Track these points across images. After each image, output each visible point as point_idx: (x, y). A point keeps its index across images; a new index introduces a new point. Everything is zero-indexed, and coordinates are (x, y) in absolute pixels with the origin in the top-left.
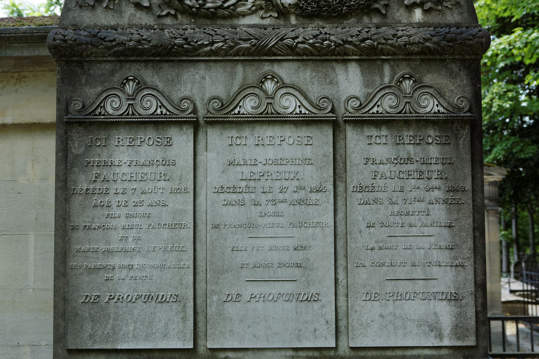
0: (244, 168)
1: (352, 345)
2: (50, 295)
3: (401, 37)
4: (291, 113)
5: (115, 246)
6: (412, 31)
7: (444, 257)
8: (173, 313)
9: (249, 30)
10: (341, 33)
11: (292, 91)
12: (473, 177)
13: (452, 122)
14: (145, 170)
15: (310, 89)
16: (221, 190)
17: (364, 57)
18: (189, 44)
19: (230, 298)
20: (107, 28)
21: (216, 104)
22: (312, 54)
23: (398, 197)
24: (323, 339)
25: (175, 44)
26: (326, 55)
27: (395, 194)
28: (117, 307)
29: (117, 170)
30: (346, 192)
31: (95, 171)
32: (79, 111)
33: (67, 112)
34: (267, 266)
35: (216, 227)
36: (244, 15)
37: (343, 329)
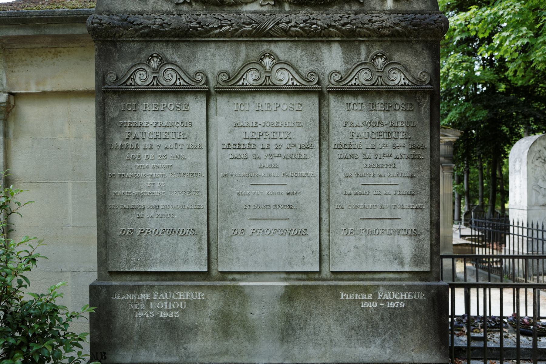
0: (247, 129)
1: (332, 269)
3: (375, 22)
4: (285, 85)
5: (145, 190)
6: (385, 17)
7: (407, 201)
8: (192, 244)
10: (326, 19)
11: (285, 66)
12: (431, 137)
13: (416, 92)
14: (168, 130)
15: (300, 65)
16: (228, 147)
17: (345, 39)
18: (202, 27)
19: (236, 233)
20: (134, 13)
21: (225, 77)
22: (302, 36)
23: (370, 153)
24: (310, 265)
25: (191, 28)
26: (314, 37)
27: (368, 151)
28: (147, 239)
29: (146, 130)
30: (329, 149)
31: (128, 130)
32: (114, 82)
33: (104, 83)
34: (265, 208)
35: (225, 176)
37: (325, 257)
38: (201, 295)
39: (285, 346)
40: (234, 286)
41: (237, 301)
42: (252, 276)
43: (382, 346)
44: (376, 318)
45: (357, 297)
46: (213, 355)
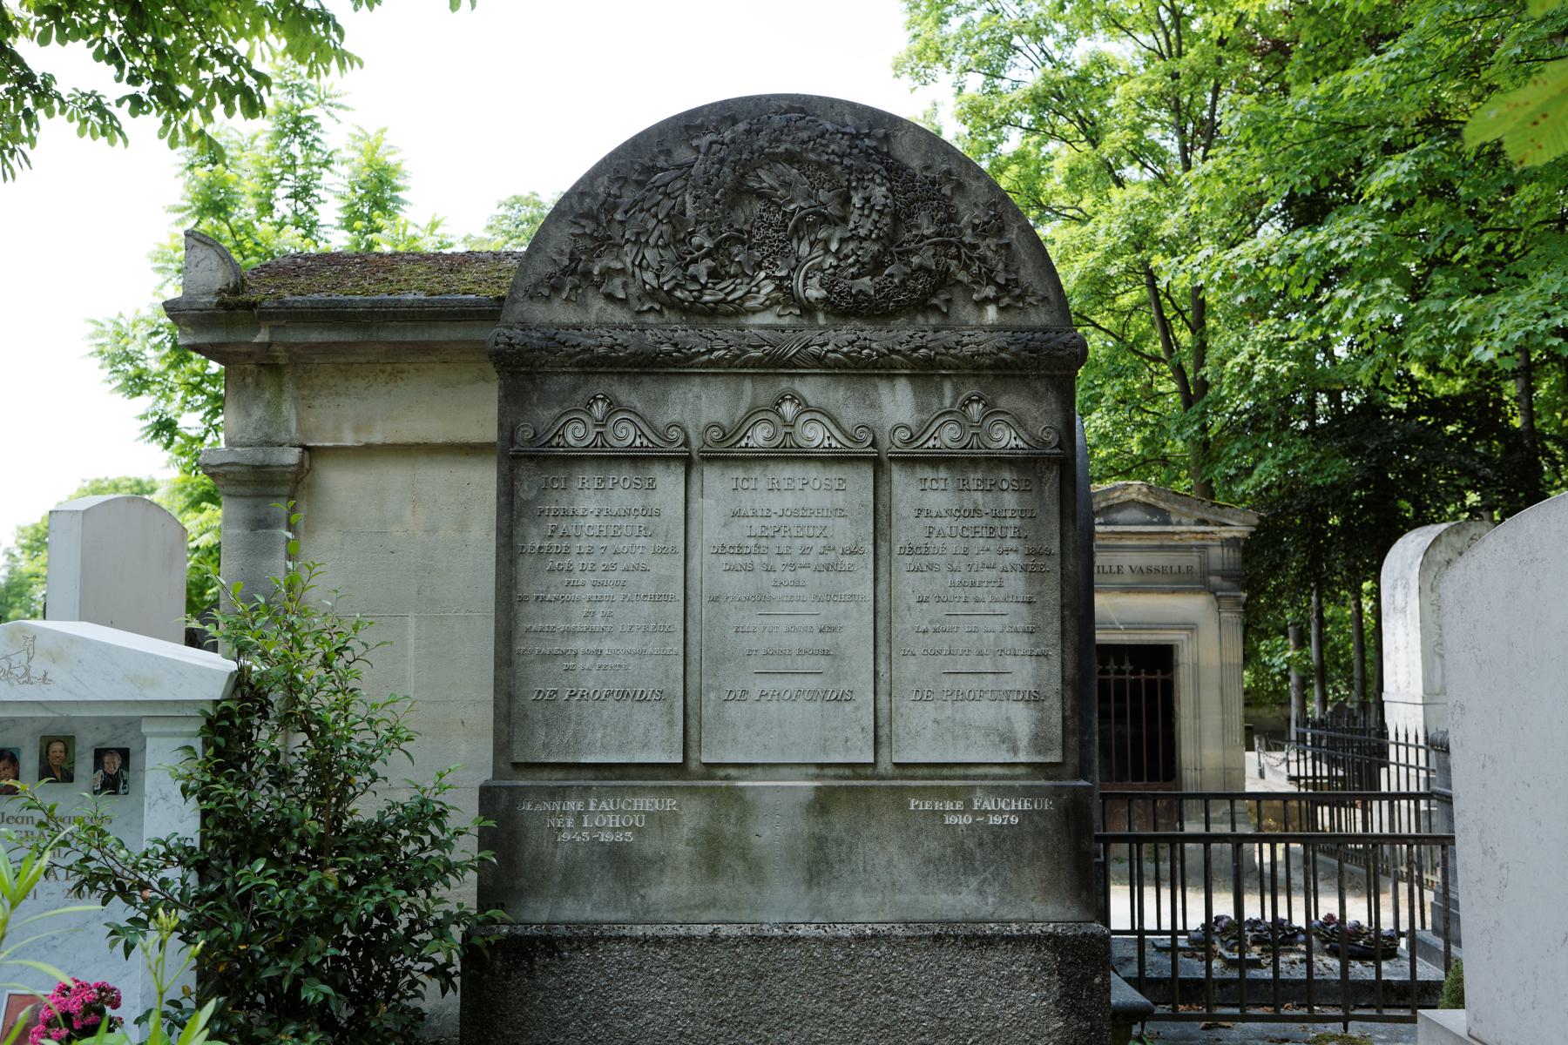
0: (753, 521)
3: (967, 345)
4: (817, 447)
5: (578, 624)
6: (982, 337)
7: (1021, 643)
8: (656, 716)
9: (761, 332)
10: (886, 339)
11: (818, 416)
13: (1035, 461)
14: (619, 522)
15: (843, 414)
16: (721, 550)
17: (917, 372)
18: (679, 351)
19: (732, 696)
20: (567, 327)
21: (716, 434)
22: (846, 367)
24: (857, 752)
25: (661, 352)
26: (865, 368)
28: (580, 707)
29: (582, 522)
30: (890, 554)
31: (551, 522)
32: (530, 441)
33: (512, 442)
34: (782, 654)
35: (715, 600)
36: (754, 311)
37: (884, 739)
38: (670, 803)
39: (815, 892)
40: (728, 788)
41: (733, 815)
42: (759, 770)
43: (981, 892)
44: (970, 844)
45: (938, 806)
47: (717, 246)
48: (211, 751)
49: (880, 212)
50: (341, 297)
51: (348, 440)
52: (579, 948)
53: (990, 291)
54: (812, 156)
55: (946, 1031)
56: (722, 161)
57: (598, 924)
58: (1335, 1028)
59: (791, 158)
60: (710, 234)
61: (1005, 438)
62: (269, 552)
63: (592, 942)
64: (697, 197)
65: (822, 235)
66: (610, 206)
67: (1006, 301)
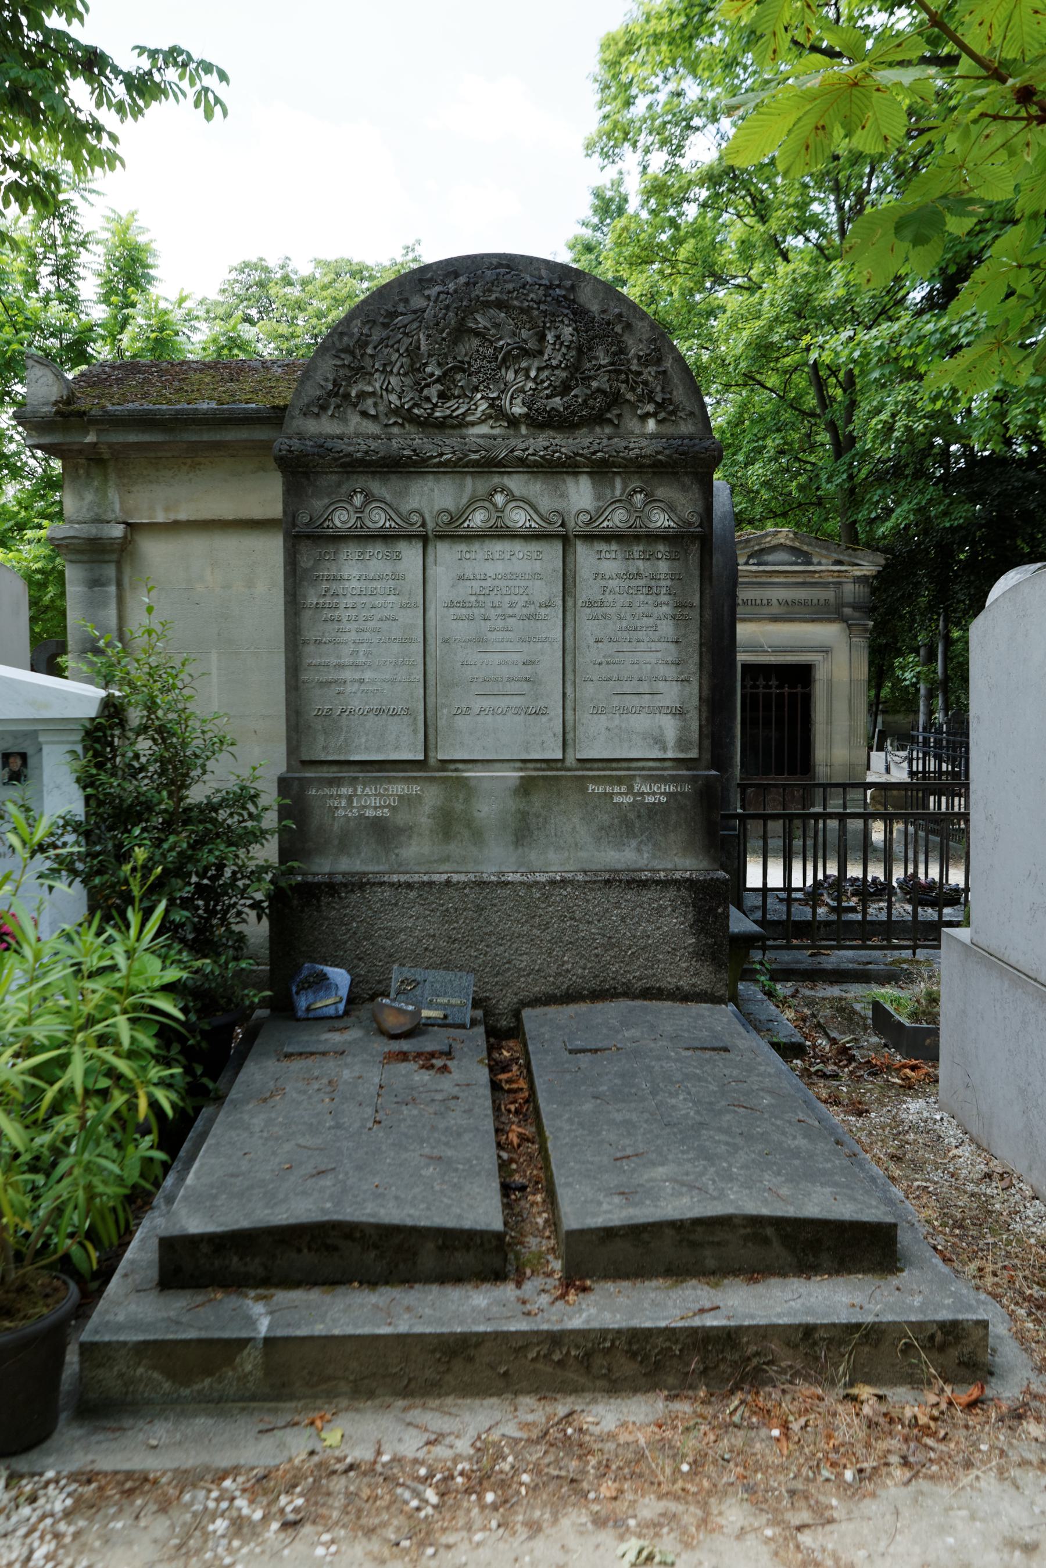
0: (474, 583)
1: (579, 757)
2: (283, 708)
5: (346, 660)
6: (644, 443)
7: (671, 672)
9: (478, 440)
11: (522, 504)
13: (683, 537)
14: (375, 584)
16: (451, 605)
21: (446, 518)
22: (542, 466)
23: (626, 612)
27: (624, 610)
29: (347, 584)
31: (325, 585)
32: (307, 524)
33: (294, 525)
34: (496, 681)
35: (446, 641)
36: (473, 424)
37: (570, 742)
38: (416, 789)
39: (520, 850)
40: (457, 778)
41: (461, 796)
42: (479, 765)
43: (639, 850)
44: (632, 816)
45: (609, 789)
46: (431, 862)
47: (445, 374)
48: (90, 753)
49: (568, 347)
50: (151, 407)
51: (160, 518)
52: (352, 891)
53: (650, 408)
54: (516, 303)
55: (613, 946)
56: (447, 307)
57: (365, 874)
58: (907, 954)
59: (500, 305)
60: (439, 365)
61: (660, 520)
62: (104, 604)
63: (362, 886)
64: (429, 336)
65: (523, 365)
66: (363, 344)
67: (662, 415)
